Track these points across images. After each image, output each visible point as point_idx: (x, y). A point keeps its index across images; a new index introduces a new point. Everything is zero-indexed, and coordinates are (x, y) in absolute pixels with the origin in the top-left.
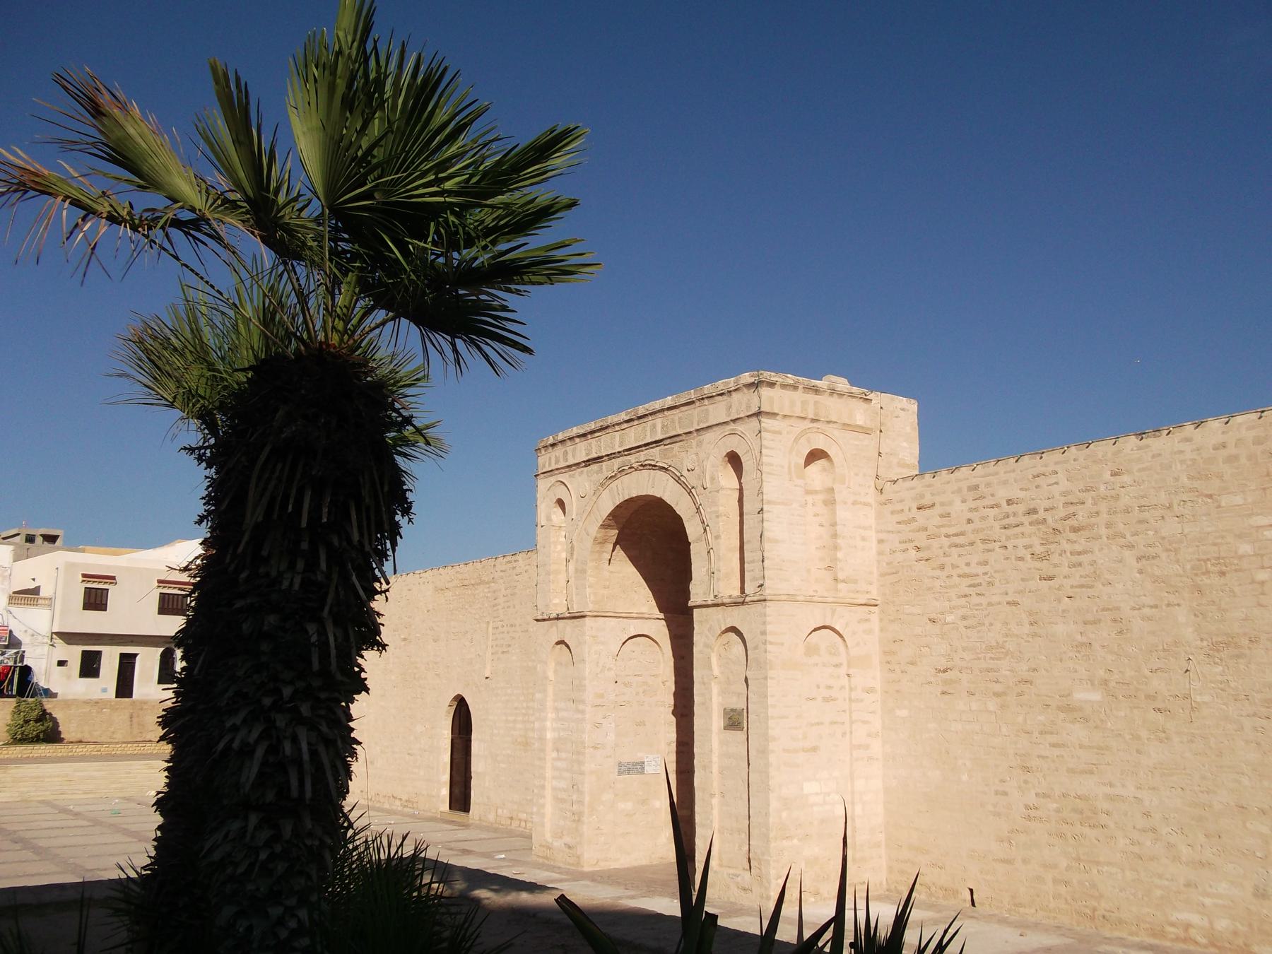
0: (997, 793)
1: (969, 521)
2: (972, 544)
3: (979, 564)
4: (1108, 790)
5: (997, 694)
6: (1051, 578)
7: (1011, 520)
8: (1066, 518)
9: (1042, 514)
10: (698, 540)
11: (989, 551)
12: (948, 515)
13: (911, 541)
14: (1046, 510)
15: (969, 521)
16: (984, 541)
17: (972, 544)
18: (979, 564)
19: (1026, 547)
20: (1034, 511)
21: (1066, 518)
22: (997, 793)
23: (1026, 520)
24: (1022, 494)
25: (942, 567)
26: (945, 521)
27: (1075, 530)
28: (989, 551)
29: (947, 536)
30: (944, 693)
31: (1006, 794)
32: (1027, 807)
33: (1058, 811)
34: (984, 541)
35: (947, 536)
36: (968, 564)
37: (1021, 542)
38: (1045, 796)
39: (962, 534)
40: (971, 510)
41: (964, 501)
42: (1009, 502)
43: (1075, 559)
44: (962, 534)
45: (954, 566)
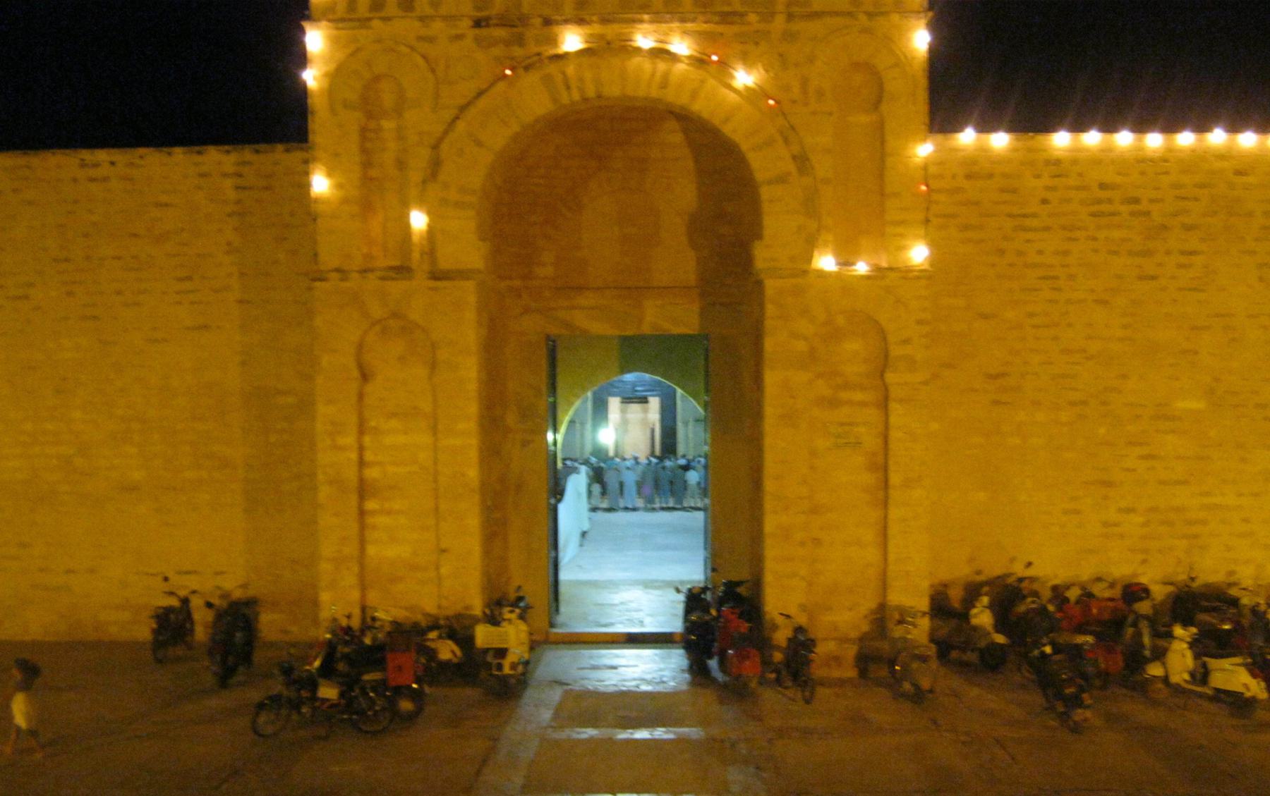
0: (1066, 512)
1: (1045, 201)
2: (1047, 229)
3: (1057, 253)
4: (1206, 500)
5: (1072, 404)
6: (1153, 278)
7: (1105, 208)
8: (1175, 215)
9: (1144, 206)
10: (782, 179)
11: (1070, 239)
12: (1014, 191)
13: (953, 216)
14: (1152, 201)
15: (1045, 201)
16: (1064, 228)
17: (1047, 229)
18: (1057, 253)
19: (1123, 240)
20: (1136, 201)
21: (1175, 215)
22: (1066, 512)
23: (1124, 209)
24: (1119, 179)
25: (1002, 252)
26: (1006, 197)
27: (1188, 228)
28: (1070, 239)
29: (1010, 216)
30: (996, 403)
31: (1077, 512)
32: (1106, 524)
33: (1146, 524)
34: (1064, 228)
35: (1010, 216)
36: (1040, 252)
37: (1116, 234)
38: (1130, 510)
39: (1034, 215)
40: (1048, 188)
41: (1038, 177)
42: (1103, 186)
43: (1183, 260)
44: (1034, 215)
45: (1020, 253)
